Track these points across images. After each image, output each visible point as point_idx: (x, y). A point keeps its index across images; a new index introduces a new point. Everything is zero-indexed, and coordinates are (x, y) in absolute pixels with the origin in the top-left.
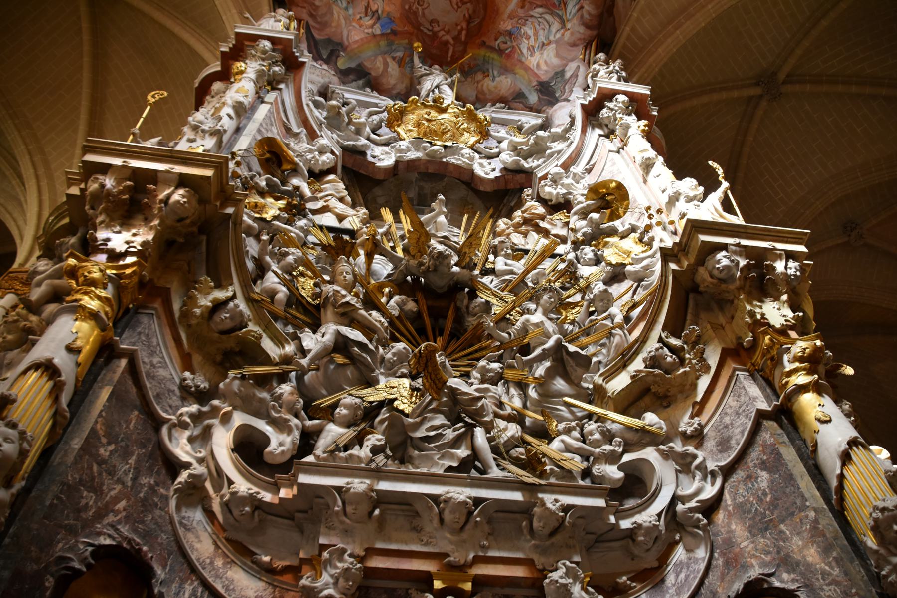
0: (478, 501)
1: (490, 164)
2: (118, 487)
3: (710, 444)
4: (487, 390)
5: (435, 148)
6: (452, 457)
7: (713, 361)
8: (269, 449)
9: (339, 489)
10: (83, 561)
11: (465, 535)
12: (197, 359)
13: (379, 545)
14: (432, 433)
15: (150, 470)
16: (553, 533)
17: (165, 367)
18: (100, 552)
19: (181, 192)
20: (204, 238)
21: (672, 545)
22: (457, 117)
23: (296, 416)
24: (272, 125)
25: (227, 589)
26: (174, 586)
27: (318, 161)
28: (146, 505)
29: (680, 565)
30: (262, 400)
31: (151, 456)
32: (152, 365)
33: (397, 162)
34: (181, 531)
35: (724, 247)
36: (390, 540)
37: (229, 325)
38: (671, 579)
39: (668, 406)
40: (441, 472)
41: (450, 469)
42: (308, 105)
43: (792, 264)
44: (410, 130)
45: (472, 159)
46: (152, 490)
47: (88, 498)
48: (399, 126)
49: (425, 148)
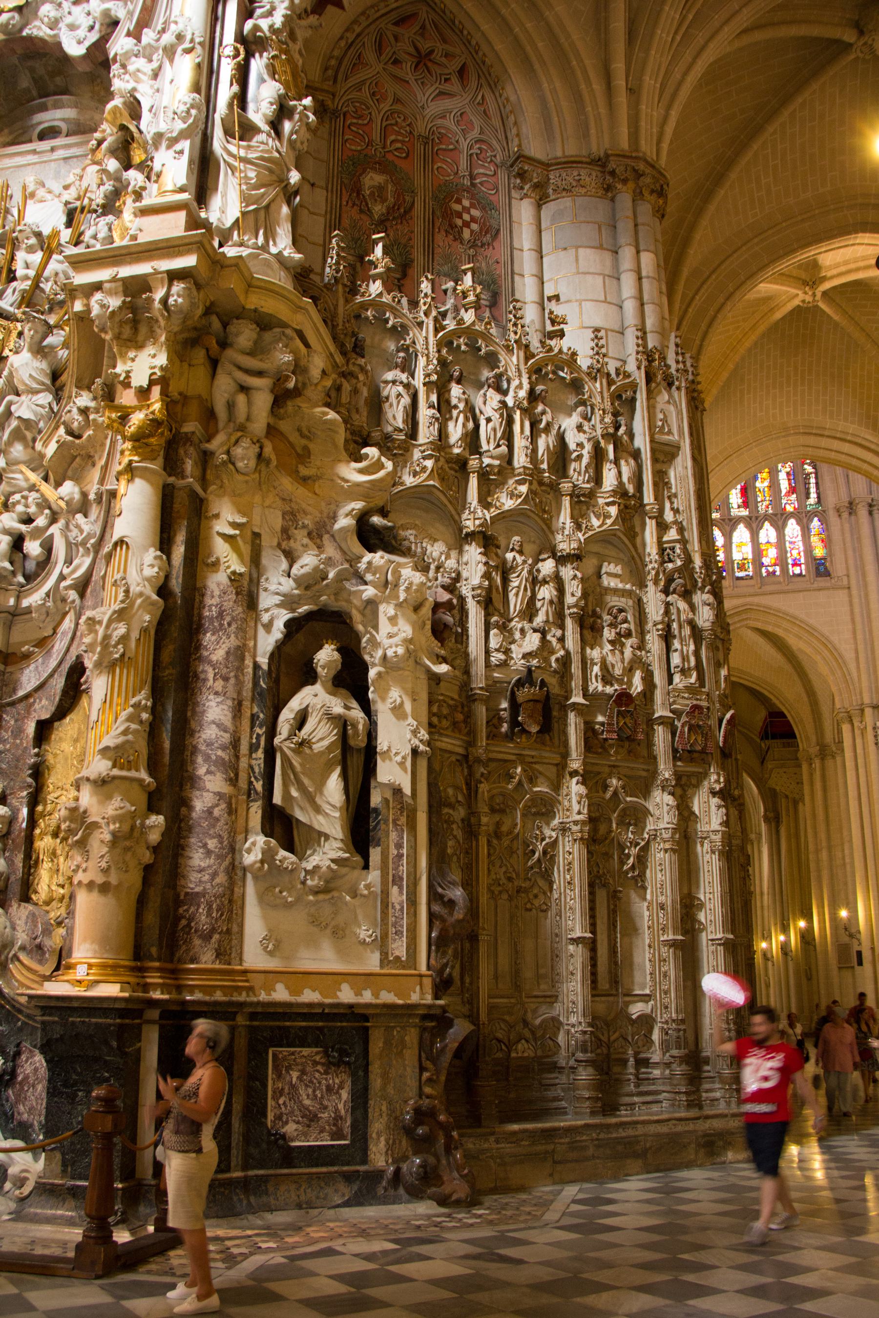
38: (56, 647)
43: (178, 287)
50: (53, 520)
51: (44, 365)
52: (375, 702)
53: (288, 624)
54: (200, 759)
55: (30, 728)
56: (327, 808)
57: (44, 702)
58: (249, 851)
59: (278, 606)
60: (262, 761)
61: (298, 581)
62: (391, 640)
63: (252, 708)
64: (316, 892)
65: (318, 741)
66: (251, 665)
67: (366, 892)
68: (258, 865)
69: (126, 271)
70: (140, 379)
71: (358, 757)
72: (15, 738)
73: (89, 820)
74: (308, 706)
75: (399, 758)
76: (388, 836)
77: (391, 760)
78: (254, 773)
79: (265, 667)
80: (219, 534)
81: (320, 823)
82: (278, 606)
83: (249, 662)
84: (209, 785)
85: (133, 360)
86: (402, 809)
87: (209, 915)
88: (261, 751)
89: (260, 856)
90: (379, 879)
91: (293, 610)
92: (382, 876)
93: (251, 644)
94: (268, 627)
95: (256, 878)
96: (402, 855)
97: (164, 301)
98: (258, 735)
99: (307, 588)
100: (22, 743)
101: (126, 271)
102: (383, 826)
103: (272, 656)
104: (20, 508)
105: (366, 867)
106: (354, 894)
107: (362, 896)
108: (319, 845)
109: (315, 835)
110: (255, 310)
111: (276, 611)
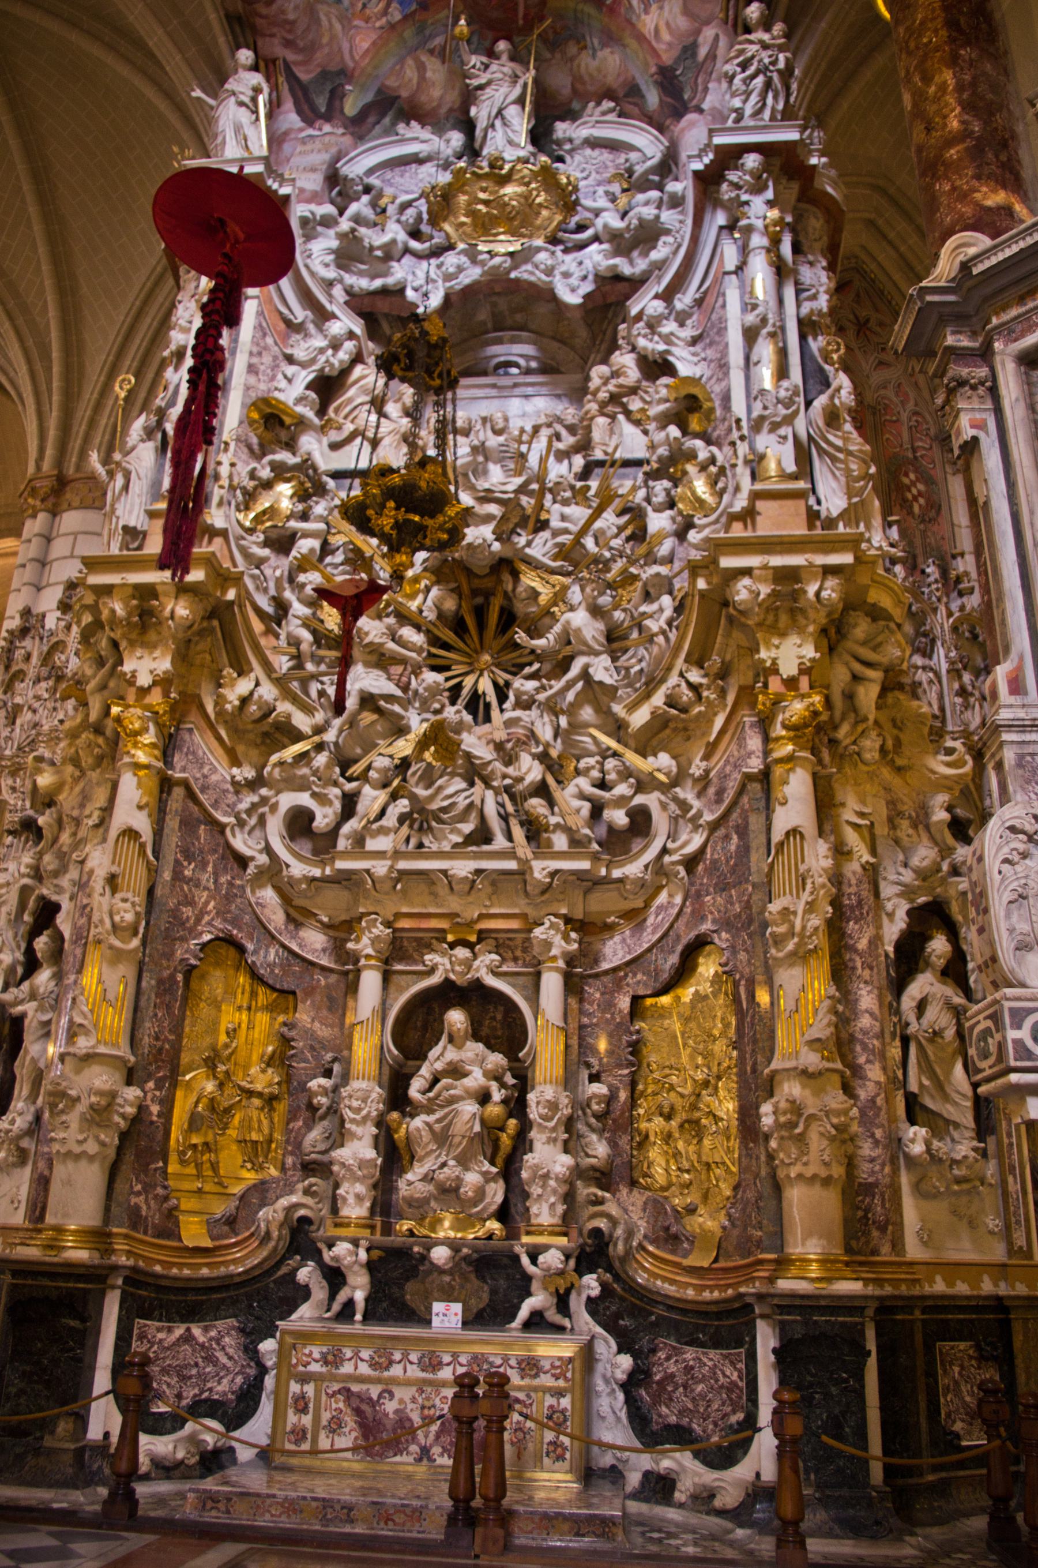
0: (478, 872)
1: (580, 263)
2: (205, 894)
3: (711, 791)
4: (519, 719)
5: (497, 260)
6: (459, 832)
7: (731, 698)
8: (315, 824)
9: (368, 871)
10: (196, 957)
11: (470, 899)
12: (240, 749)
13: (405, 910)
14: (445, 803)
15: (225, 870)
16: (543, 892)
17: (214, 770)
18: (204, 946)
19: (182, 603)
20: (215, 623)
21: (659, 889)
22: (527, 184)
23: (336, 784)
24: (265, 335)
25: (300, 946)
26: (262, 953)
27: (332, 365)
28: (229, 898)
29: (661, 908)
30: (303, 777)
31: (223, 857)
32: (205, 777)
33: (447, 298)
34: (258, 910)
35: (747, 572)
36: (412, 904)
37: (258, 714)
38: (651, 920)
39: (688, 739)
40: (448, 848)
41: (456, 845)
42: (307, 266)
43: (831, 582)
44: (463, 224)
45: (549, 271)
46: (230, 884)
47: (187, 912)
48: (445, 220)
49: (483, 263)
50: (640, 787)
51: (601, 626)
54: (858, 1048)
55: (624, 1003)
56: (957, 1098)
57: (639, 976)
59: (898, 895)
61: (917, 871)
69: (777, 561)
70: (789, 668)
72: (604, 1012)
73: (807, 1112)
80: (848, 822)
82: (898, 895)
84: (870, 1074)
85: (777, 647)
87: (883, 1206)
94: (891, 916)
97: (817, 594)
99: (924, 880)
100: (613, 1018)
101: (777, 561)
103: (899, 946)
104: (595, 774)
110: (874, 605)
111: (895, 900)
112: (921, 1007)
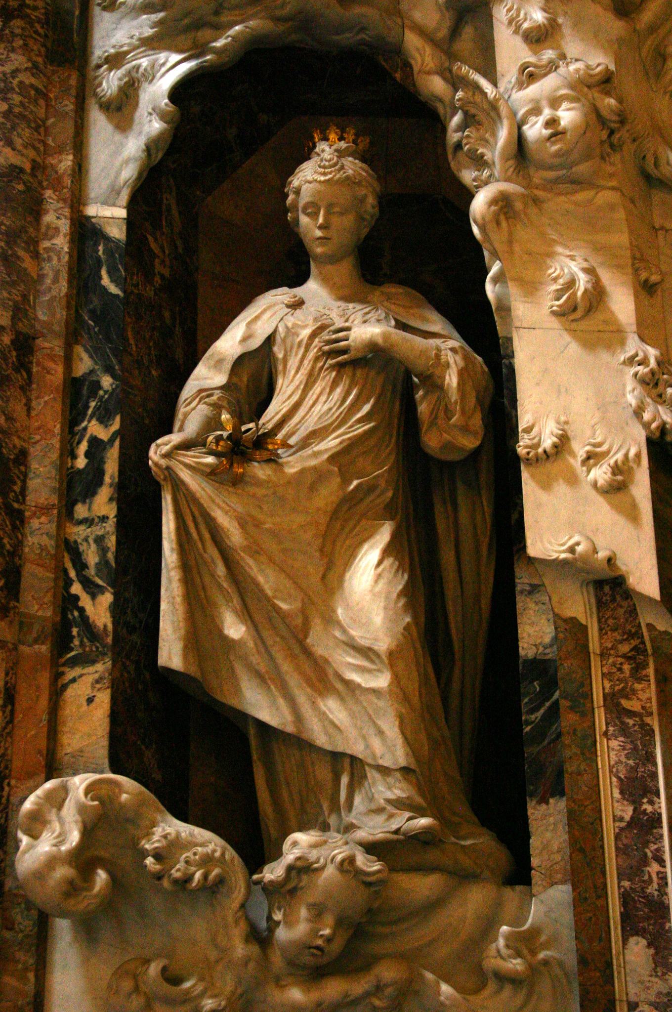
52: (505, 309)
53: (178, 93)
56: (349, 668)
58: (36, 824)
59: (151, 44)
60: (110, 526)
62: (533, 90)
63: (68, 360)
64: (315, 967)
65: (305, 443)
66: (64, 226)
67: (516, 965)
68: (62, 872)
71: (452, 484)
74: (270, 340)
75: (601, 474)
76: (589, 751)
77: (573, 480)
78: (80, 565)
79: (117, 233)
81: (333, 723)
83: (56, 219)
86: (637, 658)
88: (104, 493)
89: (74, 837)
90: (567, 917)
91: (196, 50)
92: (579, 902)
93: (66, 162)
94: (122, 108)
95: (88, 929)
96: (656, 820)
98: (95, 442)
102: (568, 720)
105: (519, 874)
106: (476, 977)
107: (503, 978)
108: (335, 806)
109: (323, 772)
112: (256, 376)
